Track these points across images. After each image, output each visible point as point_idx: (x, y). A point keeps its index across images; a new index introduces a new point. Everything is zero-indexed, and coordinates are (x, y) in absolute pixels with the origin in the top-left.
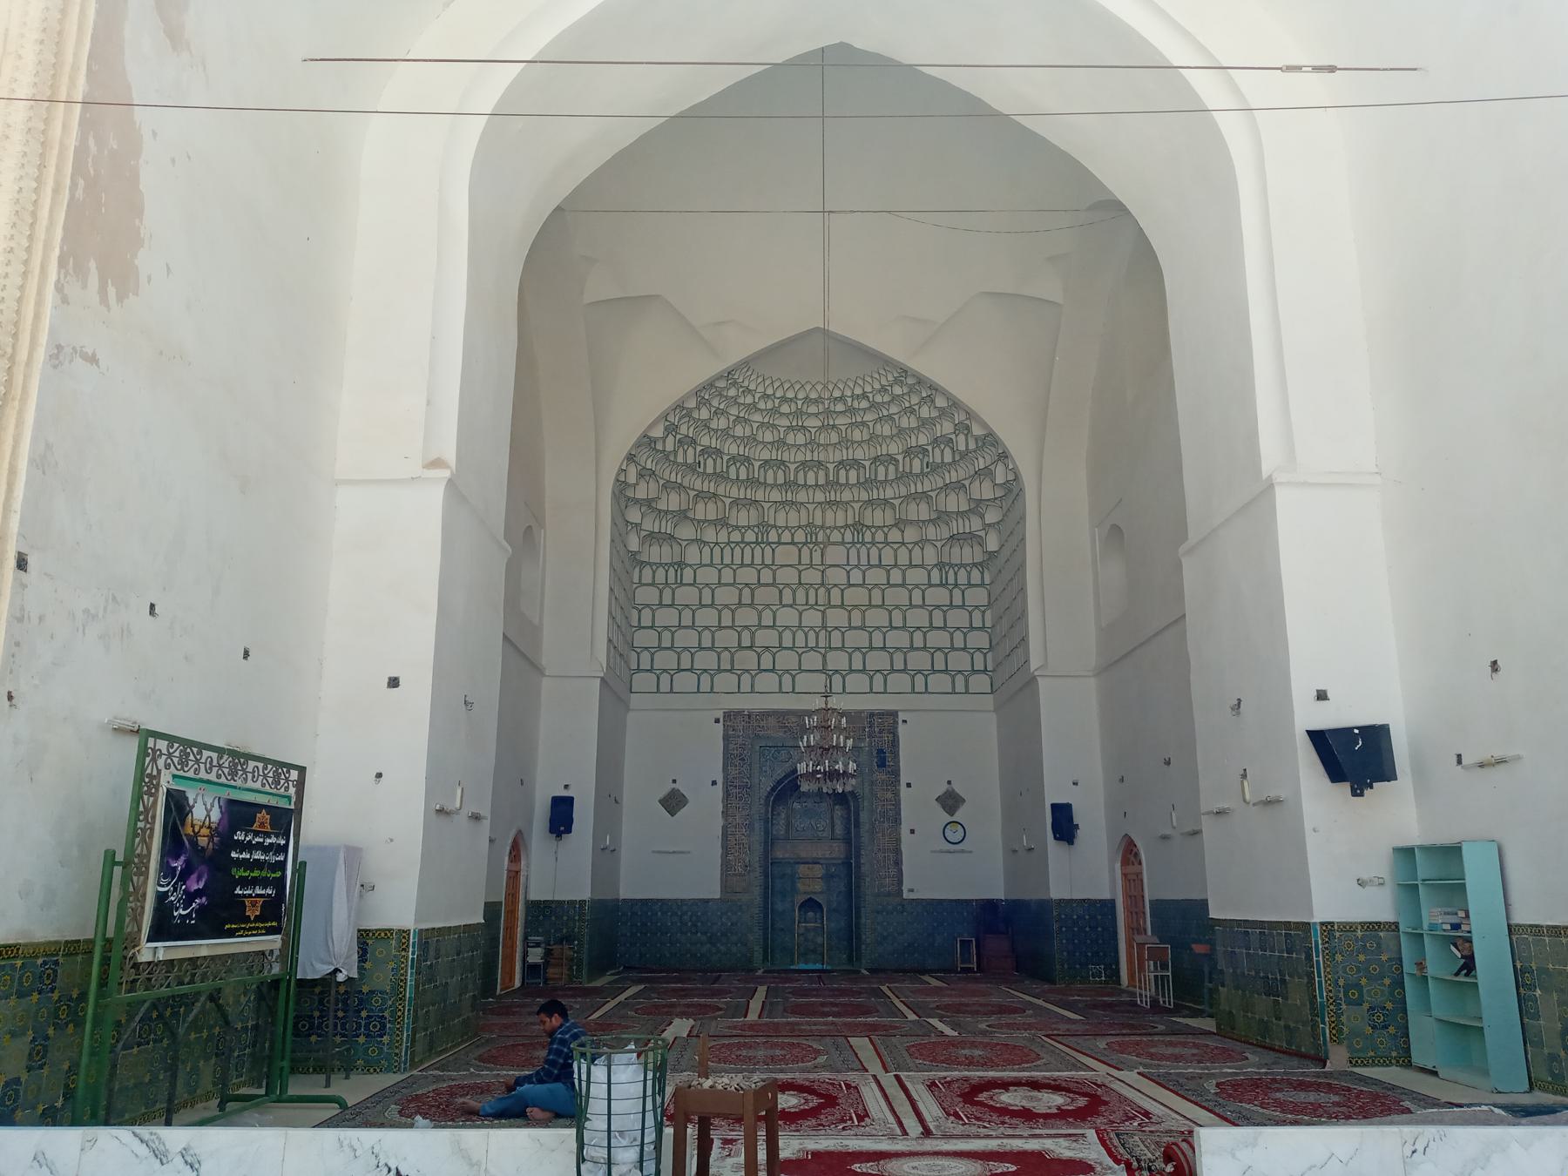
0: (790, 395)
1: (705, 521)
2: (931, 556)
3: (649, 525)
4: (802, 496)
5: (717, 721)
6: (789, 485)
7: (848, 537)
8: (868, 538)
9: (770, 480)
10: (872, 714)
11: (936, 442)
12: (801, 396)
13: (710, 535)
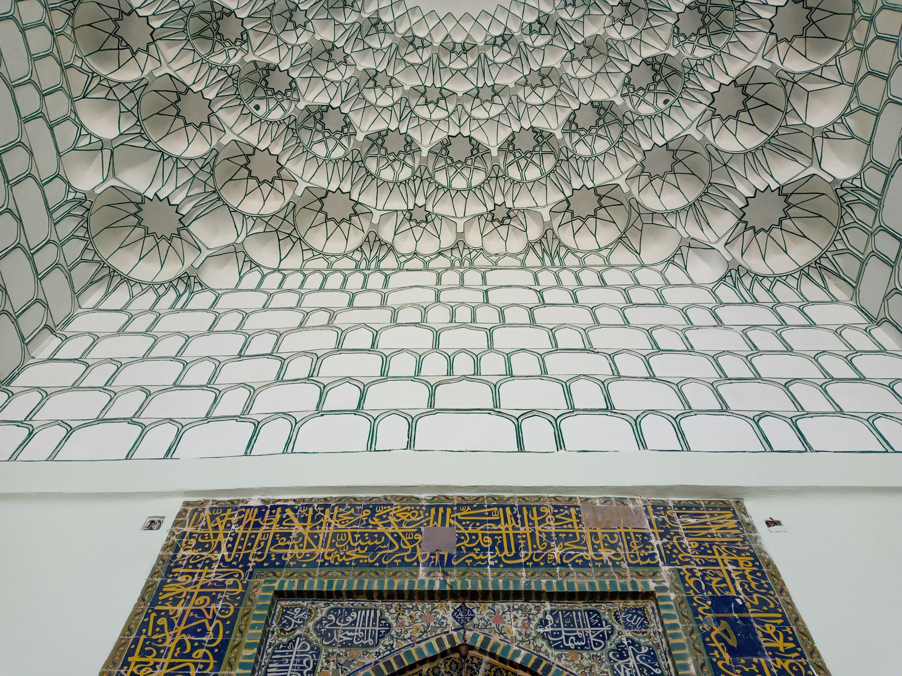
0: (421, 33)
1: (260, 217)
2: (705, 270)
3: (137, 179)
4: (444, 208)
5: (153, 524)
6: (421, 177)
7: (532, 260)
8: (571, 260)
9: (387, 174)
10: (659, 507)
11: (676, 32)
12: (438, 40)
13: (266, 255)
